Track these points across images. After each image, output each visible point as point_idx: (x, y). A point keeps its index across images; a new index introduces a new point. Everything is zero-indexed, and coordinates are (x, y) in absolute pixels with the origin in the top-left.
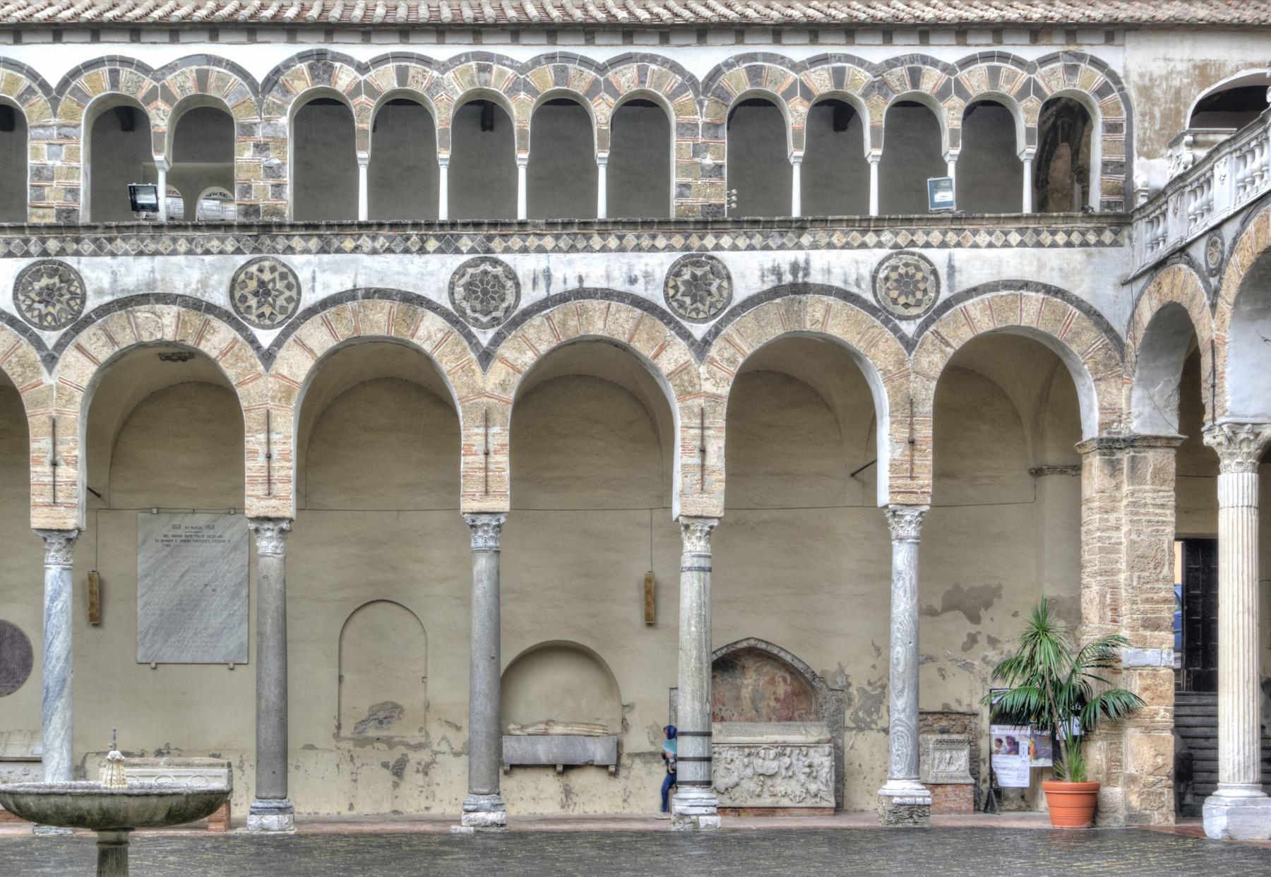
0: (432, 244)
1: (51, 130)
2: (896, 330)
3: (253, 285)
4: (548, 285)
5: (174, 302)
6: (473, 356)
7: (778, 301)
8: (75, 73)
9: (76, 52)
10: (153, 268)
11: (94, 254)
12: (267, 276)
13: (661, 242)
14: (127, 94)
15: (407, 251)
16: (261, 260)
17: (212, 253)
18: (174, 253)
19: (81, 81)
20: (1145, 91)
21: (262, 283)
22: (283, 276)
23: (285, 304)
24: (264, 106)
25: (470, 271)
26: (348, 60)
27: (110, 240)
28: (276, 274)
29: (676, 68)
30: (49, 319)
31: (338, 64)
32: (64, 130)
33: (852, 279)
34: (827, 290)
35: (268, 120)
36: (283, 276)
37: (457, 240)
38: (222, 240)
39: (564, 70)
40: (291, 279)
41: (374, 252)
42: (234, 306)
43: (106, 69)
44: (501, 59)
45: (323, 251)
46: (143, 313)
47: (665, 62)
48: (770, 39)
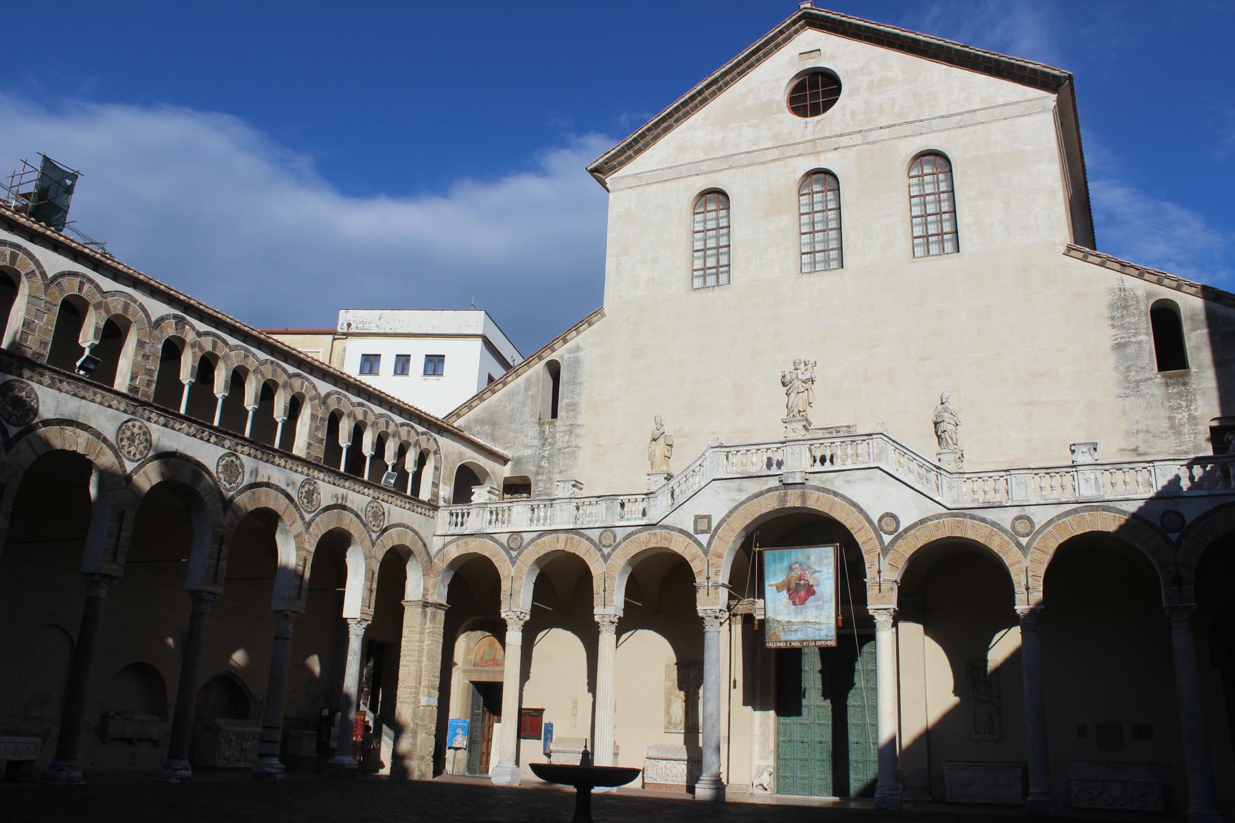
0: (213, 439)
1: (40, 301)
2: (370, 536)
3: (128, 433)
4: (256, 477)
5: (86, 430)
6: (221, 505)
7: (335, 511)
8: (62, 275)
9: (66, 264)
10: (80, 406)
11: (49, 386)
12: (136, 430)
13: (300, 469)
14: (86, 298)
15: (202, 439)
16: (135, 420)
17: (112, 408)
18: (93, 401)
19: (65, 281)
20: (446, 457)
21: (133, 434)
22: (145, 433)
23: (143, 450)
24: (152, 335)
25: (227, 458)
26: (193, 328)
27: (61, 381)
28: (141, 431)
29: (315, 388)
30: (14, 418)
31: (187, 327)
32: (48, 305)
33: (360, 508)
34: (351, 511)
35: (153, 343)
36: (145, 433)
37: (224, 440)
38: (119, 403)
39: (276, 370)
40: (148, 436)
41: (188, 434)
42: (117, 443)
43: (79, 279)
44: (254, 355)
45: (165, 425)
46: (69, 430)
47: (312, 383)
48: (345, 387)
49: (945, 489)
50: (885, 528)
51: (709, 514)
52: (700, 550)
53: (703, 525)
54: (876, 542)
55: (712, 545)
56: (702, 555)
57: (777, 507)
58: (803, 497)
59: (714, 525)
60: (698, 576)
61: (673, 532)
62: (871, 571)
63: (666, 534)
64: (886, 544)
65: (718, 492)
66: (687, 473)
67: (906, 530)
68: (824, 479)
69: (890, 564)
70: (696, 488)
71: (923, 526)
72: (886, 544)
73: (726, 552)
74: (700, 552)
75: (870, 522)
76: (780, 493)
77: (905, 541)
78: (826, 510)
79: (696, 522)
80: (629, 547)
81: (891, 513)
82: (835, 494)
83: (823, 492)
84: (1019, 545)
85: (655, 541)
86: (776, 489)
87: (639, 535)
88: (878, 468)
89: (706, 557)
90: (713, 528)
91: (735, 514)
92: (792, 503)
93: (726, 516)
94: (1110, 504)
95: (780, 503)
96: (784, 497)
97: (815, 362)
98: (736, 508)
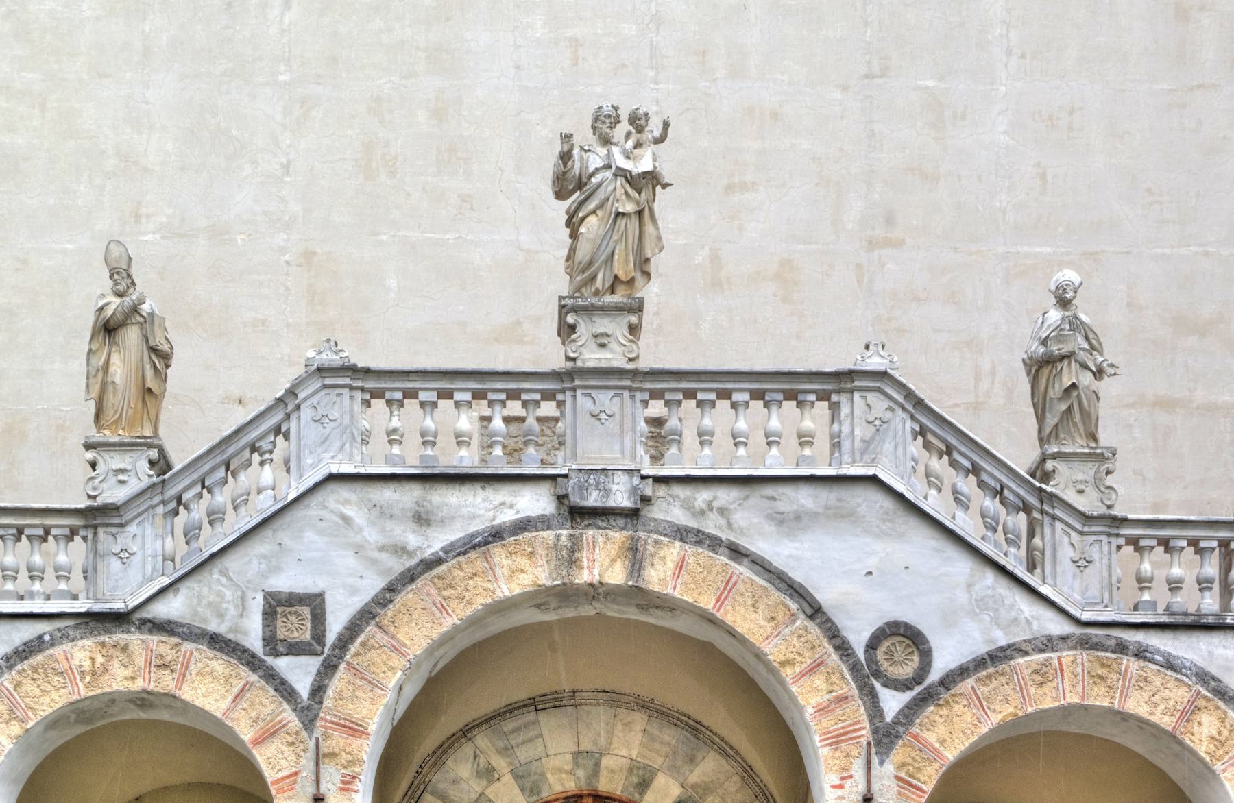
49: (1065, 566)
50: (885, 665)
51: (314, 590)
52: (285, 706)
53: (296, 628)
55: (330, 692)
58: (635, 556)
59: (335, 626)
60: (280, 791)
61: (188, 646)
63: (165, 650)
64: (889, 717)
66: (231, 450)
69: (898, 778)
70: (265, 504)
71: (1000, 668)
72: (889, 717)
73: (376, 719)
74: (288, 715)
75: (843, 648)
76: (558, 538)
77: (944, 711)
79: (270, 614)
80: (30, 688)
81: (907, 626)
82: (736, 552)
83: (699, 543)
85: (128, 673)
86: (543, 522)
87: (67, 646)
90: (331, 637)
92: (596, 572)
95: (557, 568)
96: (572, 551)
97: (666, 125)
98: (409, 577)
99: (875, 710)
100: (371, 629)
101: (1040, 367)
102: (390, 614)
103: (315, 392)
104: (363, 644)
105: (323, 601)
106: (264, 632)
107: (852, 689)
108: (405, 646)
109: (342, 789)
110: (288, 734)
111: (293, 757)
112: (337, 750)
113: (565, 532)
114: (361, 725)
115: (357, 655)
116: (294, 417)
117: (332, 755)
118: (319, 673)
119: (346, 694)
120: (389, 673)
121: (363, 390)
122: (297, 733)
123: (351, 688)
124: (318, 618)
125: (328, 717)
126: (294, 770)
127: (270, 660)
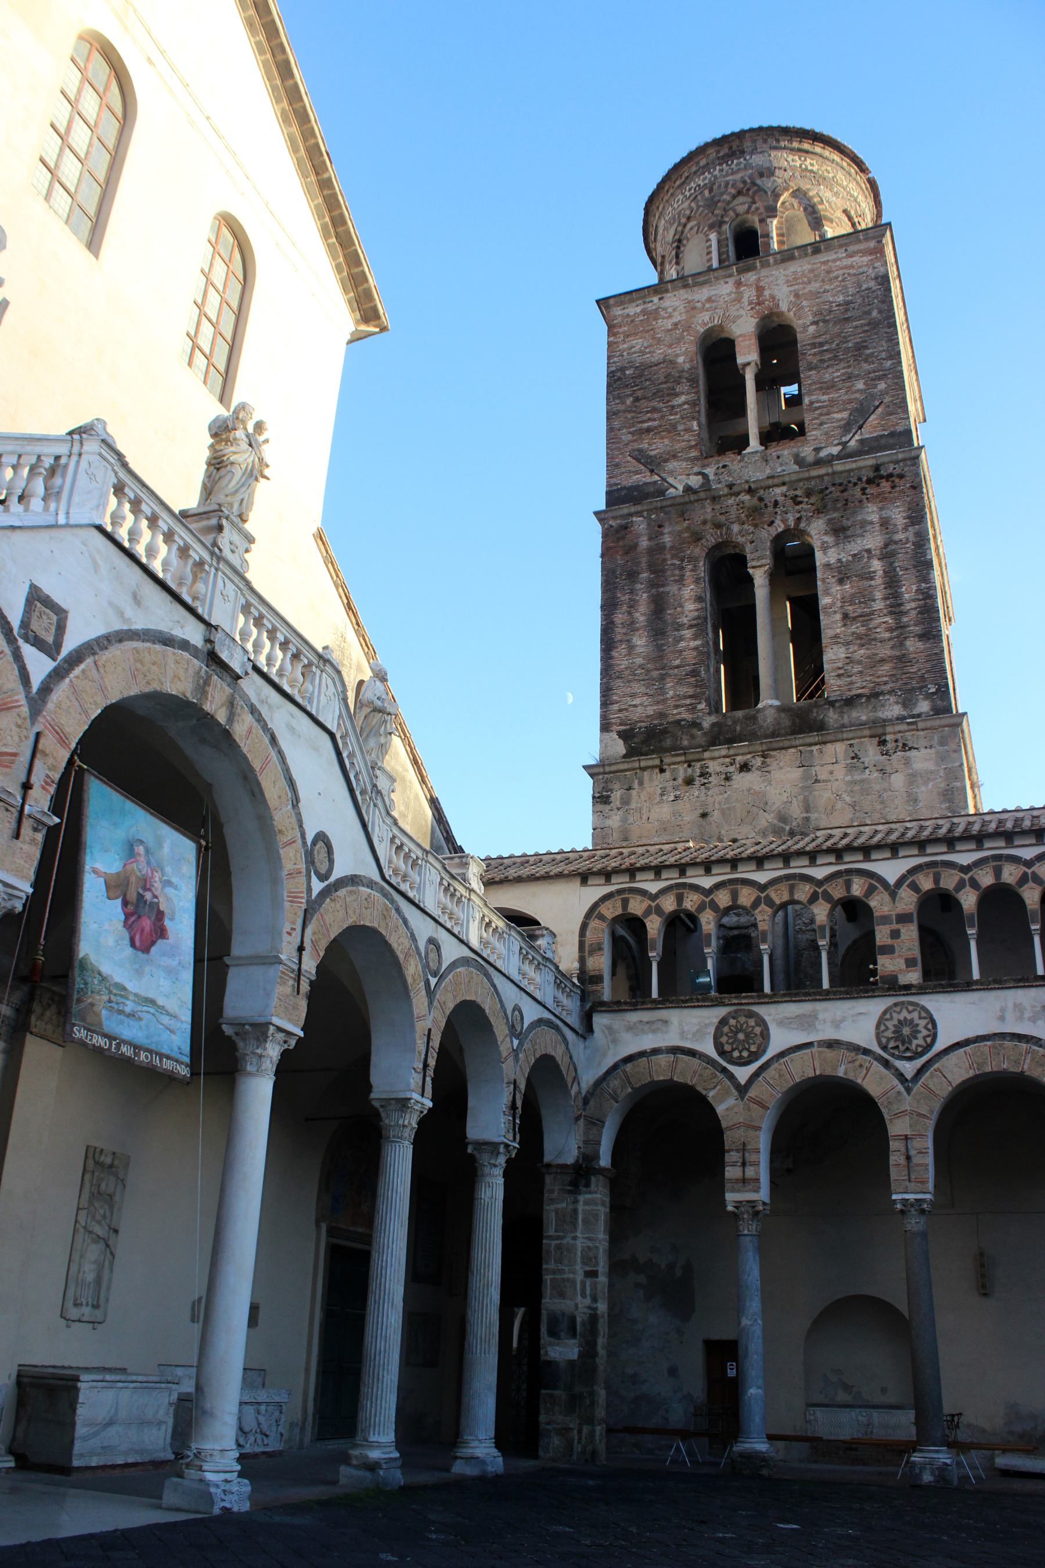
50: (316, 861)
54: (303, 880)
56: (25, 710)
57: (188, 695)
59: (70, 644)
62: (289, 942)
65: (96, 568)
67: (341, 883)
68: (263, 696)
69: (312, 942)
74: (21, 698)
78: (256, 765)
82: (273, 740)
84: (427, 983)
86: (194, 651)
88: (332, 736)
89: (33, 724)
90: (65, 652)
91: (115, 651)
93: (97, 640)
94: (491, 970)
99: (309, 889)
100: (89, 660)
101: (374, 711)
102: (104, 658)
103: (93, 454)
104: (83, 671)
105: (66, 618)
106: (23, 616)
107: (302, 866)
108: (108, 690)
109: (43, 788)
110: (19, 715)
111: (16, 738)
112: (48, 752)
113: (205, 667)
114: (67, 739)
115: (77, 677)
116: (74, 458)
117: (45, 754)
118: (49, 676)
119: (64, 706)
120: (93, 706)
121: (116, 473)
122: (25, 719)
123: (68, 701)
124: (61, 629)
125: (49, 719)
126: (14, 751)
127: (21, 642)
